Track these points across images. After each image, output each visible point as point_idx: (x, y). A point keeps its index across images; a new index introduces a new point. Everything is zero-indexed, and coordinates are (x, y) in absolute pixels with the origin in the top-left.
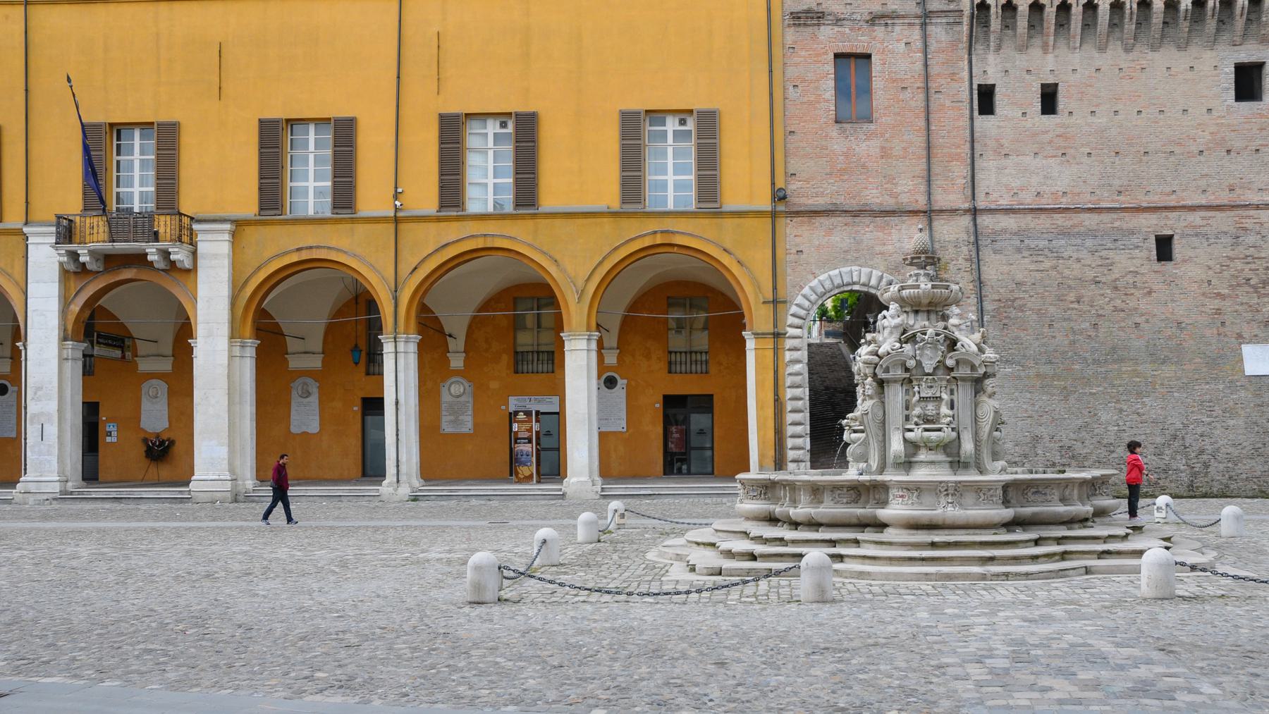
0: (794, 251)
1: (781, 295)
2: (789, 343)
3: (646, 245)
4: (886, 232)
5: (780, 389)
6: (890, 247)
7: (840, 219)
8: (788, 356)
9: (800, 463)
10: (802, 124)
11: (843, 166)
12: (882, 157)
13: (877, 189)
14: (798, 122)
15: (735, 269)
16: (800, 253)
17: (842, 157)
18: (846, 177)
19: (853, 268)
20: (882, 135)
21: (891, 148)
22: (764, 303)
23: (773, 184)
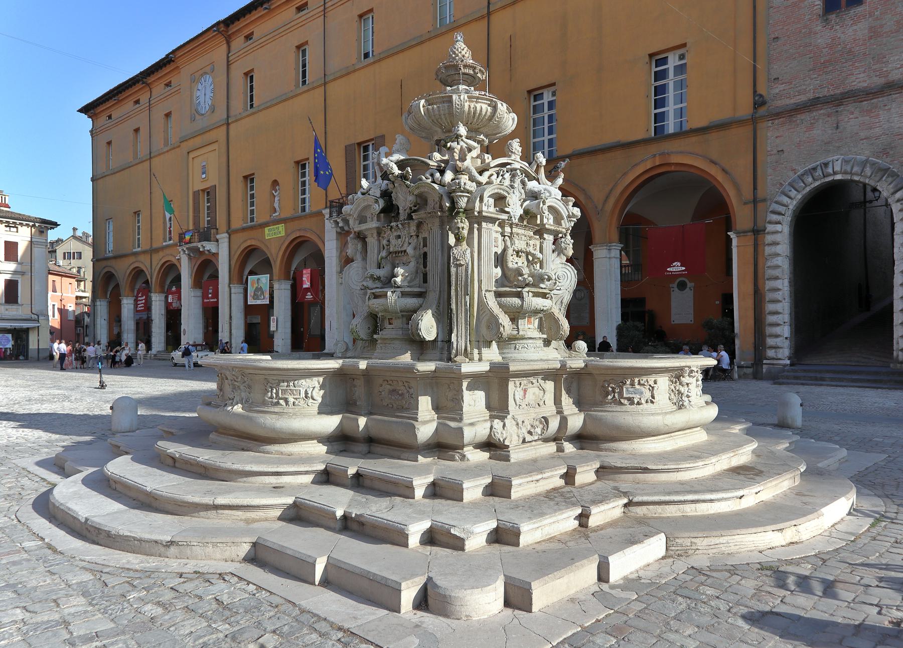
0: (775, 151)
1: (760, 194)
2: (769, 238)
3: (649, 167)
4: (872, 115)
5: (760, 282)
6: (877, 130)
7: (822, 111)
8: (768, 250)
9: (778, 350)
10: (786, 28)
11: (827, 58)
12: (870, 38)
13: (864, 72)
14: (781, 27)
15: (720, 177)
16: (780, 153)
17: (827, 49)
18: (831, 68)
19: (835, 158)
20: (871, 14)
21: (881, 26)
22: (745, 204)
23: (755, 92)
